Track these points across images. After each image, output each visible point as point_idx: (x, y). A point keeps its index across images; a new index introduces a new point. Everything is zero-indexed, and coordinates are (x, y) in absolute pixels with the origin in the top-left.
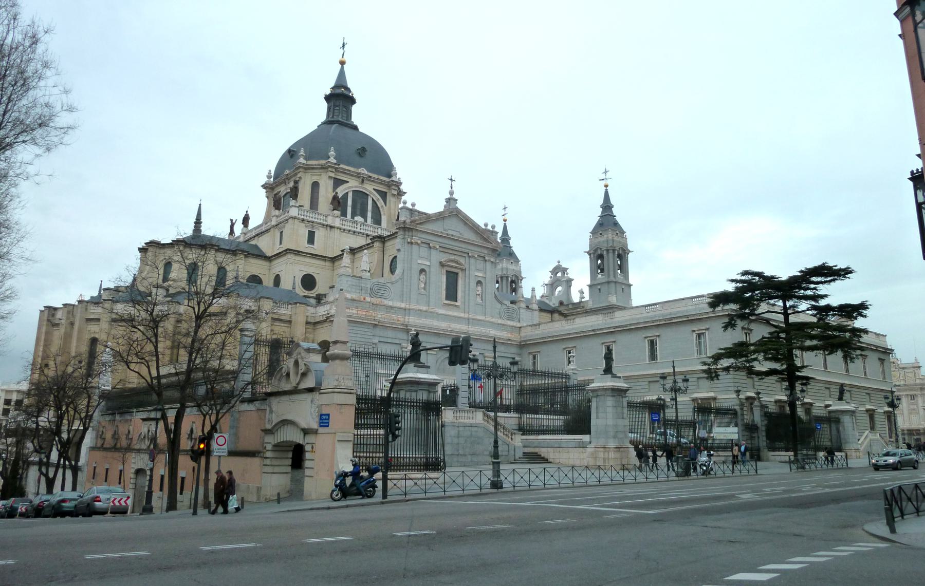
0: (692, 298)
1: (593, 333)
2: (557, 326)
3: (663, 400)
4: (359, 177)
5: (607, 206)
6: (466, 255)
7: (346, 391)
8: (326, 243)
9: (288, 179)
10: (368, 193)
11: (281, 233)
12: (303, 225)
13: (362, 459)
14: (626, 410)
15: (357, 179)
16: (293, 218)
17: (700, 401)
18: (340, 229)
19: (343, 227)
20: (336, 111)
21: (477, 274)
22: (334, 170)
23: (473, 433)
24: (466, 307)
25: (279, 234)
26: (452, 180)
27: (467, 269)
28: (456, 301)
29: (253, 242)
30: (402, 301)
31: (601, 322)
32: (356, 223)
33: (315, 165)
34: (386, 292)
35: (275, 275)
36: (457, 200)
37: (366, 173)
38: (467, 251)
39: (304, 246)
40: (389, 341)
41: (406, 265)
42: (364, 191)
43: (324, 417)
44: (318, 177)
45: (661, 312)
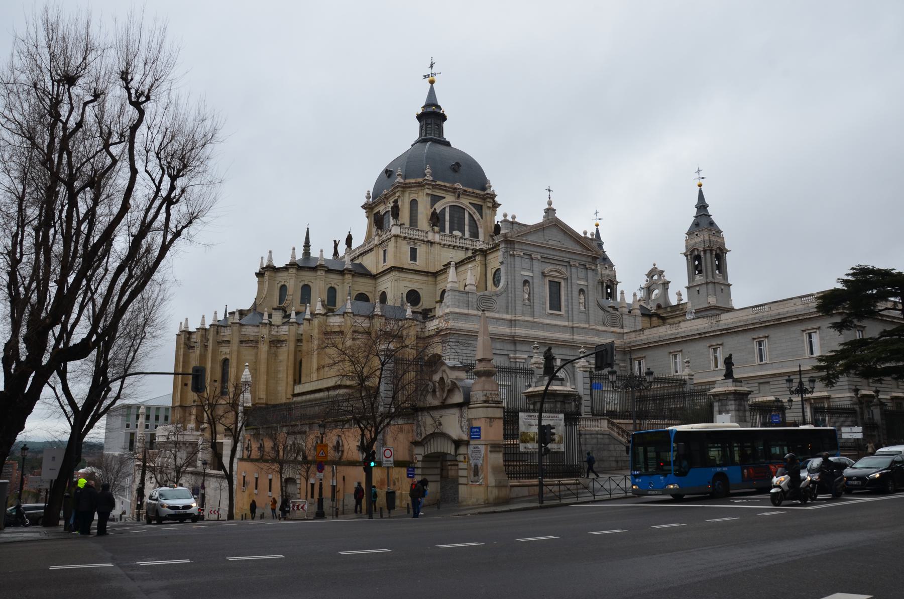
0: (801, 297)
2: (662, 330)
3: (781, 402)
5: (702, 206)
7: (494, 405)
8: (427, 259)
9: (387, 198)
10: (464, 207)
11: (385, 251)
12: (405, 242)
13: (521, 468)
14: (748, 414)
15: (453, 194)
16: (396, 236)
17: (812, 401)
18: (440, 244)
19: (443, 242)
20: (428, 129)
21: (579, 282)
22: (431, 187)
23: (599, 440)
26: (549, 190)
27: (569, 278)
29: (357, 262)
30: (507, 313)
31: (707, 325)
33: (413, 183)
34: (492, 305)
35: (380, 293)
36: (555, 210)
38: (568, 260)
39: (406, 262)
41: (509, 277)
42: (460, 205)
43: (475, 430)
44: (416, 195)
45: (770, 313)
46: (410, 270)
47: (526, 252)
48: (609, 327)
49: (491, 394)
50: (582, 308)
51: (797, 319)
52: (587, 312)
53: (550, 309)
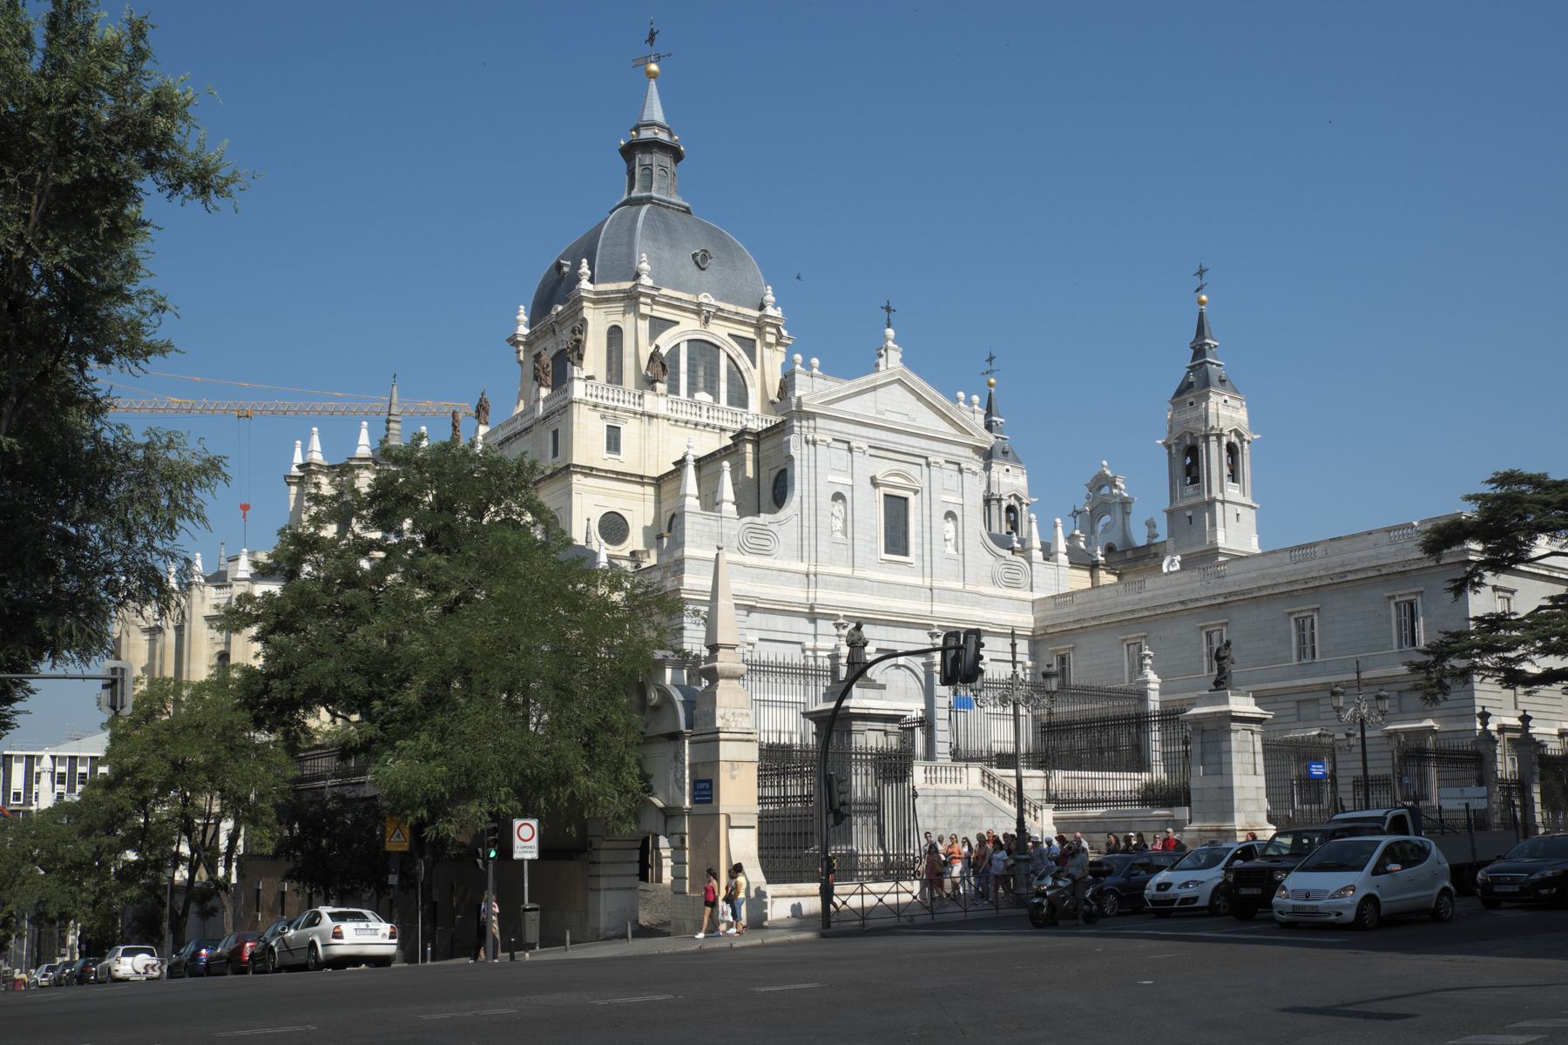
1: (1183, 608)
4: (698, 313)
6: (923, 461)
7: (739, 736)
10: (718, 343)
11: (555, 433)
12: (598, 415)
19: (674, 415)
23: (963, 808)
24: (927, 564)
25: (550, 437)
26: (888, 309)
27: (926, 491)
28: (906, 554)
31: (1198, 584)
32: (699, 405)
33: (612, 292)
34: (767, 543)
37: (713, 302)
38: (923, 453)
40: (779, 636)
43: (702, 786)
46: (606, 471)
47: (838, 436)
48: (1004, 589)
49: (734, 714)
50: (950, 550)
51: (1378, 573)
52: (960, 558)
53: (886, 552)
